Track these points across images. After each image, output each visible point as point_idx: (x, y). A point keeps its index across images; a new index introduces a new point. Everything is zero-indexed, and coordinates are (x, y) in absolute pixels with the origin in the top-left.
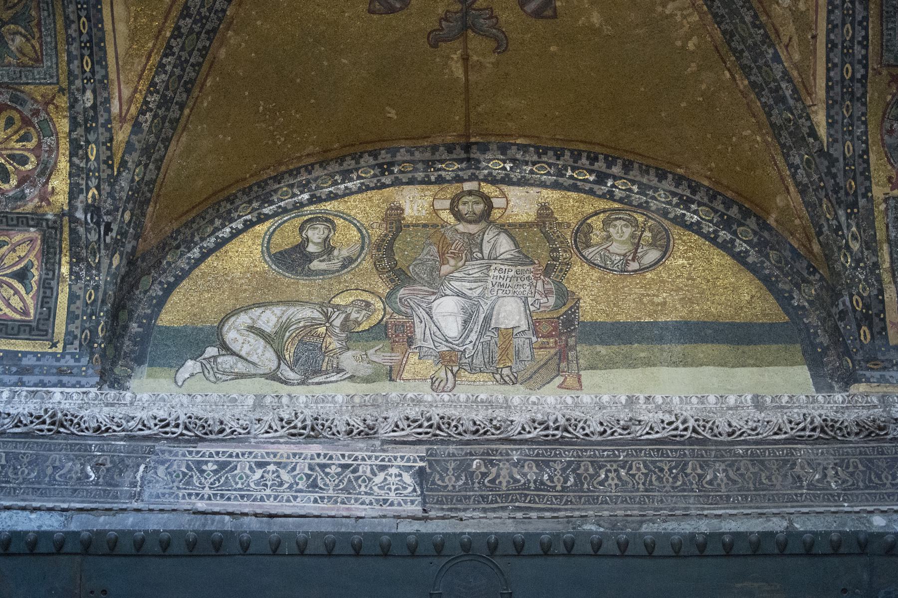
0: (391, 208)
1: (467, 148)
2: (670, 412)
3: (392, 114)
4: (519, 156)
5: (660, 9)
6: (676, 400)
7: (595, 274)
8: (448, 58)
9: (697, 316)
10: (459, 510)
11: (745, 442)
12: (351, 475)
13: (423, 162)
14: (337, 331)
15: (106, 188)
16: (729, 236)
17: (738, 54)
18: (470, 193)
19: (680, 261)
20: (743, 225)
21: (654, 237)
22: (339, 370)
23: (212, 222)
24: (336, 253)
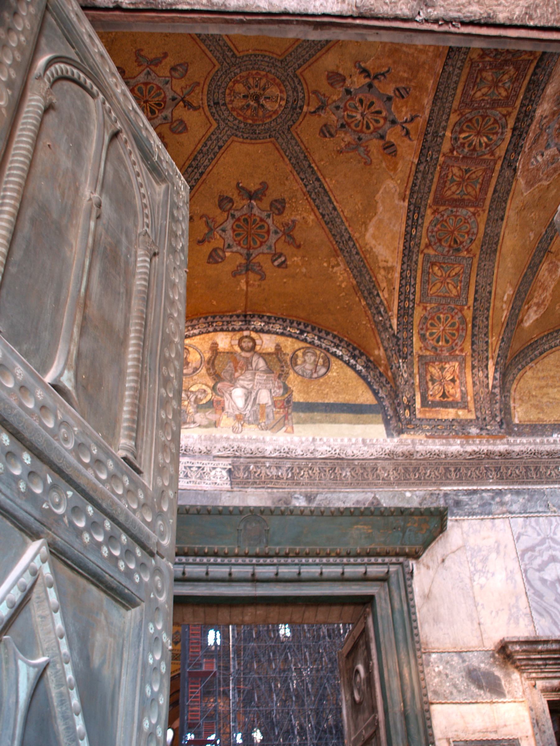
0: (213, 344)
1: (245, 316)
2: (330, 446)
3: (215, 303)
5: (330, 269)
6: (332, 440)
10: (245, 488)
11: (359, 459)
12: (202, 472)
14: (192, 403)
16: (354, 363)
17: (363, 293)
18: (246, 337)
19: (335, 374)
21: (324, 362)
22: (194, 422)
24: (190, 365)
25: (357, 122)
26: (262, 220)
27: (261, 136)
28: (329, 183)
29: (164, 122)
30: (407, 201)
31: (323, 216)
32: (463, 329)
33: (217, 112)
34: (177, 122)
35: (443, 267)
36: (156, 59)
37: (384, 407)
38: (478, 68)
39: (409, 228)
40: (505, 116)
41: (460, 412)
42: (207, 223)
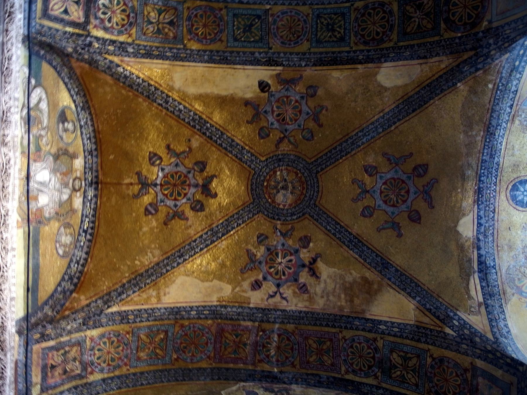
3: (112, 157)
4: (93, 201)
7: (56, 232)
8: (132, 178)
9: (41, 270)
13: (92, 167)
15: (98, 51)
18: (81, 184)
20: (71, 284)
23: (77, 87)
24: (64, 133)
25: (274, 259)
26: (185, 195)
27: (254, 192)
28: (224, 244)
29: (270, 123)
30: (218, 303)
31: (195, 241)
32: (109, 369)
33: (274, 161)
34: (267, 132)
35: (163, 341)
36: (319, 119)
37: (37, 313)
38: (333, 338)
39: (196, 309)
40: (293, 364)
41: (39, 386)
42: (183, 152)
